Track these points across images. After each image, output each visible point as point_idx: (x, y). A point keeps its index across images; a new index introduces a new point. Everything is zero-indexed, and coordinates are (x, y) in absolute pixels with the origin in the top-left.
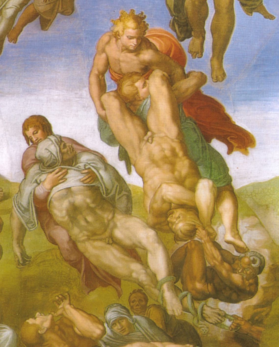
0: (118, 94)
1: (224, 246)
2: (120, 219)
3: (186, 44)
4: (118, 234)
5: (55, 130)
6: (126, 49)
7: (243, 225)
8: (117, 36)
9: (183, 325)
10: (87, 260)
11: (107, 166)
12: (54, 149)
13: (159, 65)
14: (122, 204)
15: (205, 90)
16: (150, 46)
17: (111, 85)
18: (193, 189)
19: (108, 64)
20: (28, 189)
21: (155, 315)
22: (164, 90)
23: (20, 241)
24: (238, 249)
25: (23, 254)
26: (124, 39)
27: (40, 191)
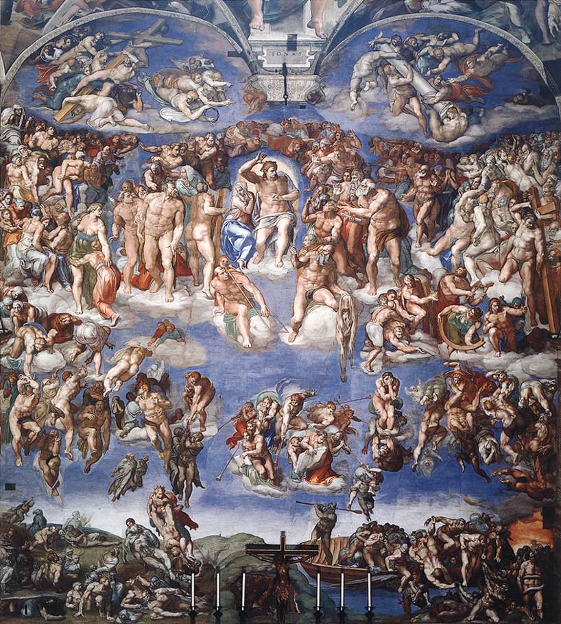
0: (156, 512)
1: (189, 558)
2: (156, 550)
3: (177, 496)
4: (155, 555)
5: (136, 523)
6: (159, 498)
7: (194, 551)
8: (156, 493)
9: (175, 582)
10: (146, 563)
11: (152, 534)
12: (136, 529)
13: (168, 502)
14: (157, 546)
15: (182, 510)
16: (167, 497)
17: (154, 509)
18: (179, 541)
19: (153, 503)
20: (127, 541)
21: (167, 579)
22: (170, 510)
23: (125, 558)
24: (193, 559)
25: (126, 561)
26: (158, 494)
27: (131, 541)
